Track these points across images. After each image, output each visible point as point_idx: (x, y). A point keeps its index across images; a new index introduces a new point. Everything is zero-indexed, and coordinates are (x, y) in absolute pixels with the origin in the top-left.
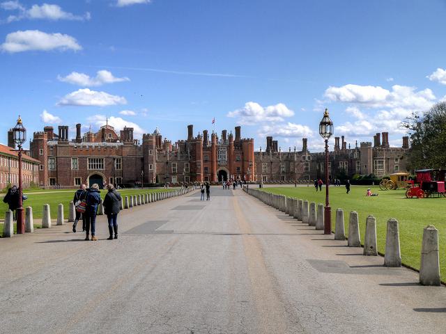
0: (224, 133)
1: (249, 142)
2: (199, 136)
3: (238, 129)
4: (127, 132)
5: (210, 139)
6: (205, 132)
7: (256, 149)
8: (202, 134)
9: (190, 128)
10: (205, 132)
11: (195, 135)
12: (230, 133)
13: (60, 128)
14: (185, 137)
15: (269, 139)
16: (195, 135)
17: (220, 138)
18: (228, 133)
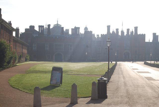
0: (128, 30)
1: (143, 36)
2: (113, 32)
3: (136, 28)
4: (76, 30)
5: (120, 34)
6: (117, 30)
7: (147, 40)
8: (115, 31)
9: (109, 27)
10: (117, 30)
11: (111, 32)
12: (131, 31)
13: (39, 26)
14: (105, 32)
15: (154, 34)
16: (111, 32)
17: (125, 34)
18: (130, 31)
